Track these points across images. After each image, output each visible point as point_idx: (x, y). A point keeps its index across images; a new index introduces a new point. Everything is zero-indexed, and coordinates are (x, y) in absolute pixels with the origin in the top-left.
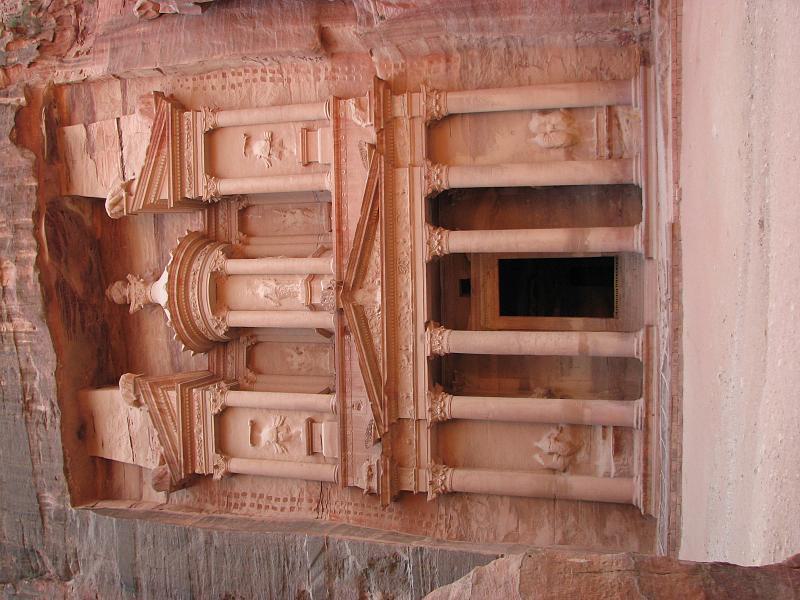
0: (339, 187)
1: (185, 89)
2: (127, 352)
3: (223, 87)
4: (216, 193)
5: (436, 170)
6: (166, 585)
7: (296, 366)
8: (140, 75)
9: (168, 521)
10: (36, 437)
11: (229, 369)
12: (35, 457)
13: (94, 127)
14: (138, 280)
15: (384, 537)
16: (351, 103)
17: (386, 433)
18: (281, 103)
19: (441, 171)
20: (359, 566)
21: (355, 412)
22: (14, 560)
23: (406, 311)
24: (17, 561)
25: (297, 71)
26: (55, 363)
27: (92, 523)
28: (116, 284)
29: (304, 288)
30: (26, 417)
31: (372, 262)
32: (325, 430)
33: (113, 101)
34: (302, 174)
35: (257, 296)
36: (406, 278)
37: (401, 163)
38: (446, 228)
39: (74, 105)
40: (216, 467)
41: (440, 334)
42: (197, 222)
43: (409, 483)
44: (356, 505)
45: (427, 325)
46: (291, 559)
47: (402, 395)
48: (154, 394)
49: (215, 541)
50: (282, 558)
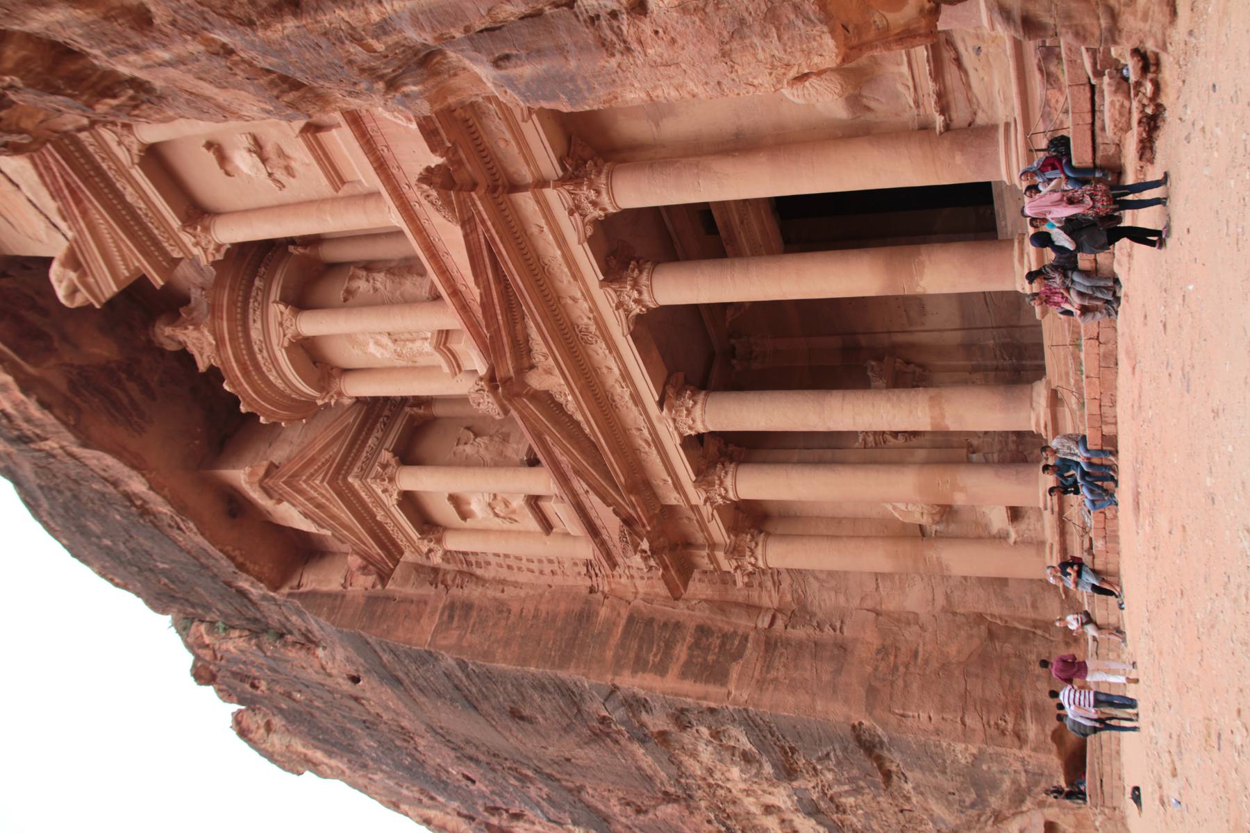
0: (420, 232)
5: (586, 193)
14: (186, 328)
19: (598, 192)
23: (622, 394)
26: (143, 480)
30: (151, 521)
32: (559, 511)
35: (374, 356)
36: (599, 350)
37: (516, 176)
40: (430, 551)
41: (687, 416)
45: (661, 404)
47: (657, 482)
48: (301, 492)
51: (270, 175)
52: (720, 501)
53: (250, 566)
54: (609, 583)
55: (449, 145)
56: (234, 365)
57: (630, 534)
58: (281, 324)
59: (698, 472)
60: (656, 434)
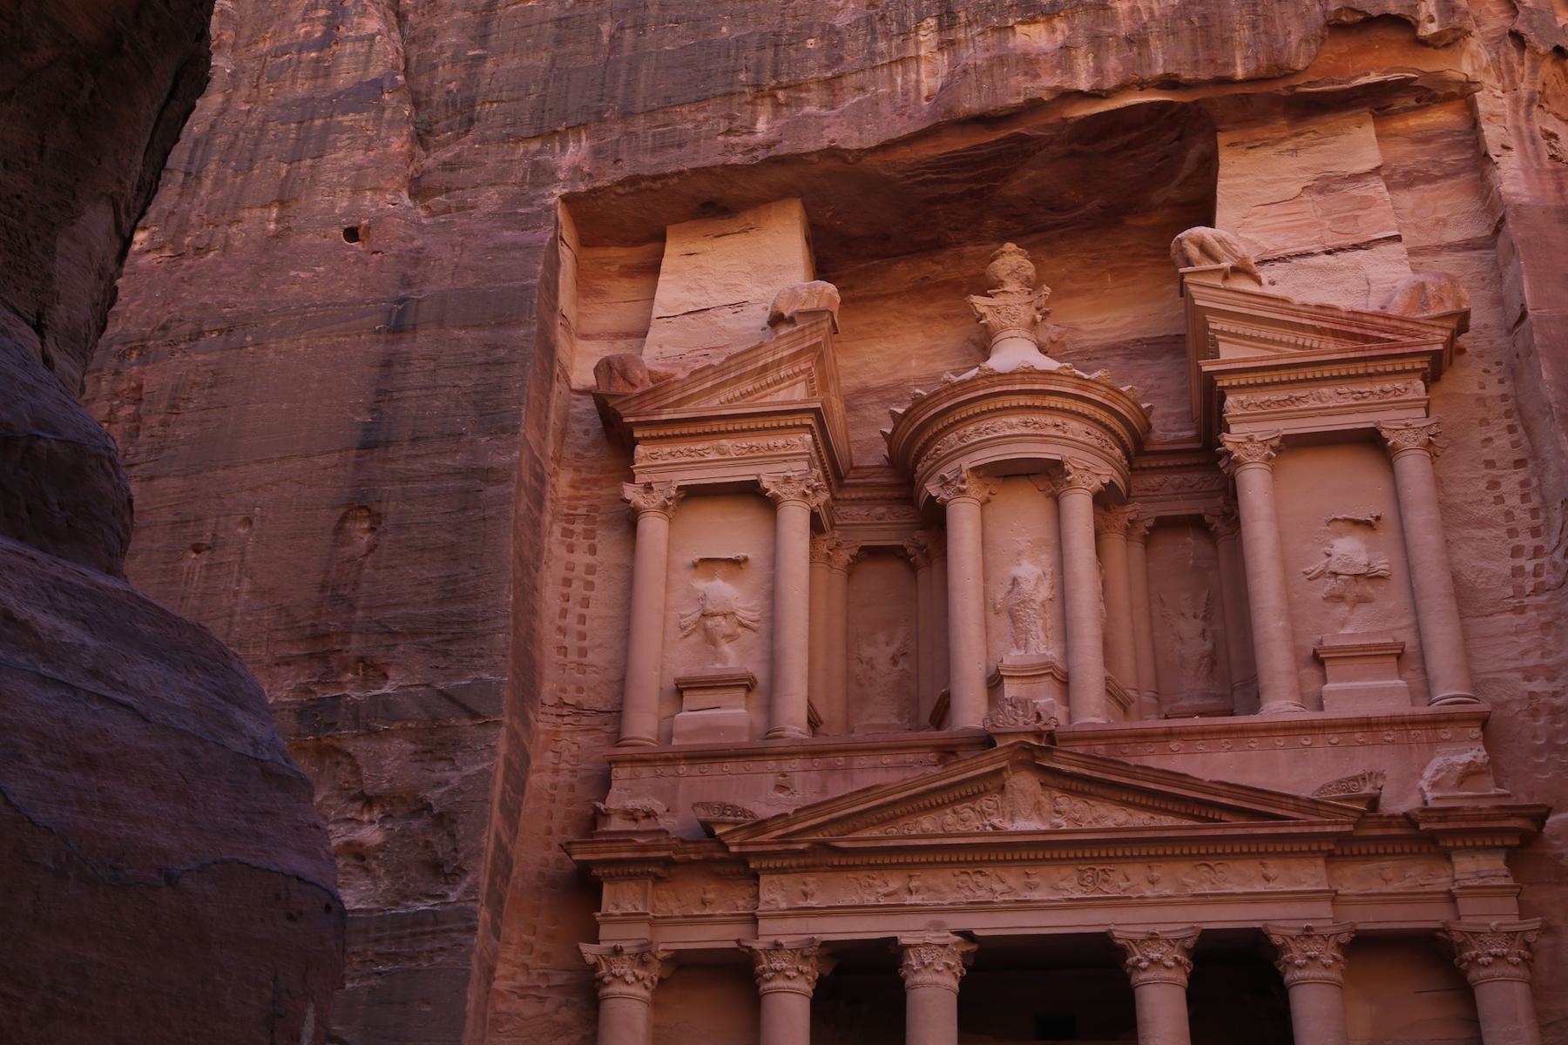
0: (1270, 730)
1: (1473, 379)
2: (887, 297)
3: (1490, 464)
4: (1238, 463)
5: (1328, 954)
6: (400, 390)
7: (867, 652)
8: (1508, 278)
9: (533, 393)
10: (701, 117)
11: (855, 510)
12: (660, 116)
13: (1377, 188)
15: (500, 847)
16: (1473, 753)
17: (726, 847)
18: (1463, 595)
20: (438, 792)
21: (771, 779)
22: (452, 86)
24: (449, 92)
25: (1545, 627)
26: (854, 145)
27: (529, 237)
28: (1028, 264)
29: (1036, 661)
31: (1101, 809)
33: (1443, 223)
34: (1296, 651)
38: (1192, 978)
39: (1427, 140)
41: (948, 967)
42: (1170, 426)
43: (619, 899)
44: (572, 788)
45: (967, 935)
46: (454, 647)
48: (796, 356)
49: (492, 489)
50: (458, 629)
51: (1336, 574)
52: (777, 965)
53: (620, 190)
54: (547, 732)
55: (1422, 827)
56: (1052, 388)
57: (736, 823)
58: (1087, 470)
59: (825, 944)
60: (909, 912)
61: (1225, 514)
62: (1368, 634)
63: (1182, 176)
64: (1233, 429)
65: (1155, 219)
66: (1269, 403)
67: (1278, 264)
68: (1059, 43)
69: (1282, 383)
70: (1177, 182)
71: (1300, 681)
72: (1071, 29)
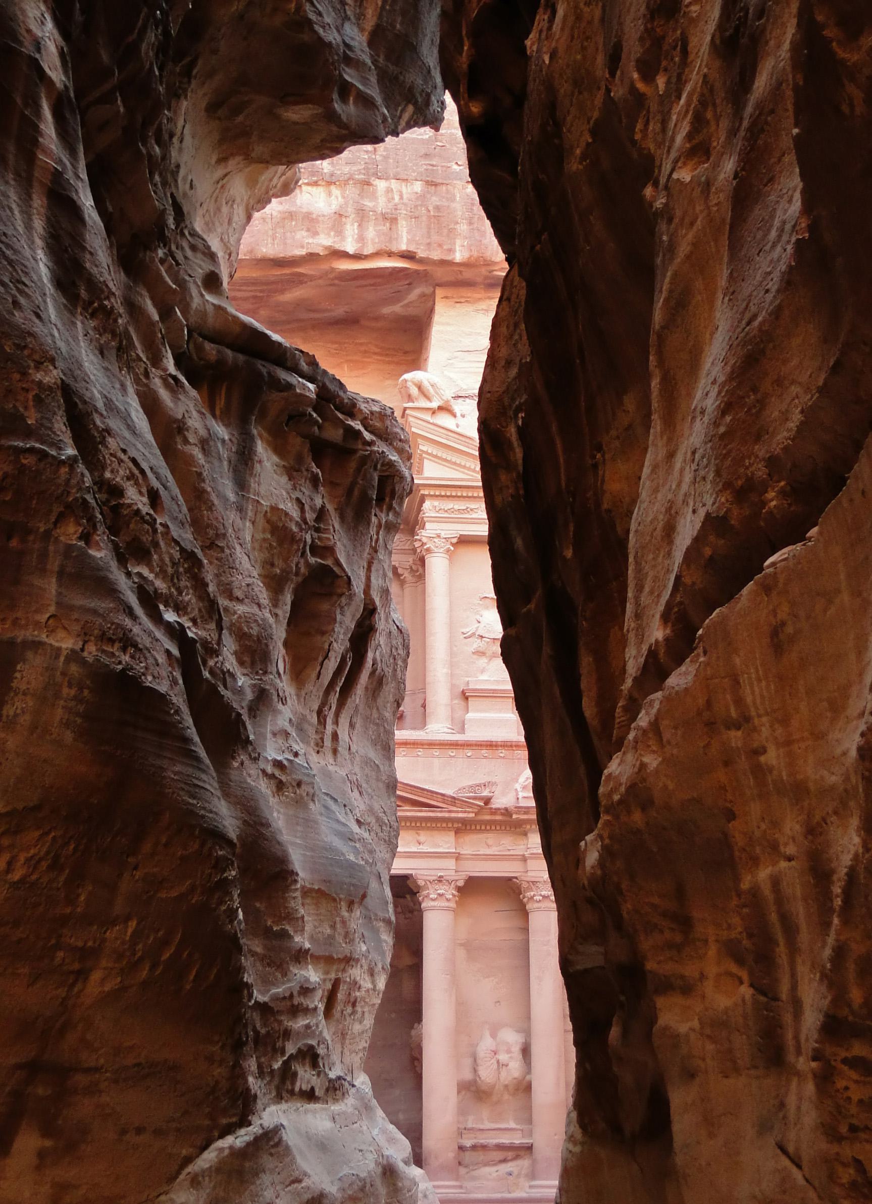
0: (431, 745)
4: (428, 550)
5: (450, 892)
51: (482, 637)
61: (411, 568)
62: (497, 682)
63: (406, 302)
64: (428, 525)
65: (379, 324)
66: (452, 511)
67: (467, 400)
68: (334, 207)
69: (462, 497)
70: (402, 304)
71: (452, 709)
72: (343, 197)
